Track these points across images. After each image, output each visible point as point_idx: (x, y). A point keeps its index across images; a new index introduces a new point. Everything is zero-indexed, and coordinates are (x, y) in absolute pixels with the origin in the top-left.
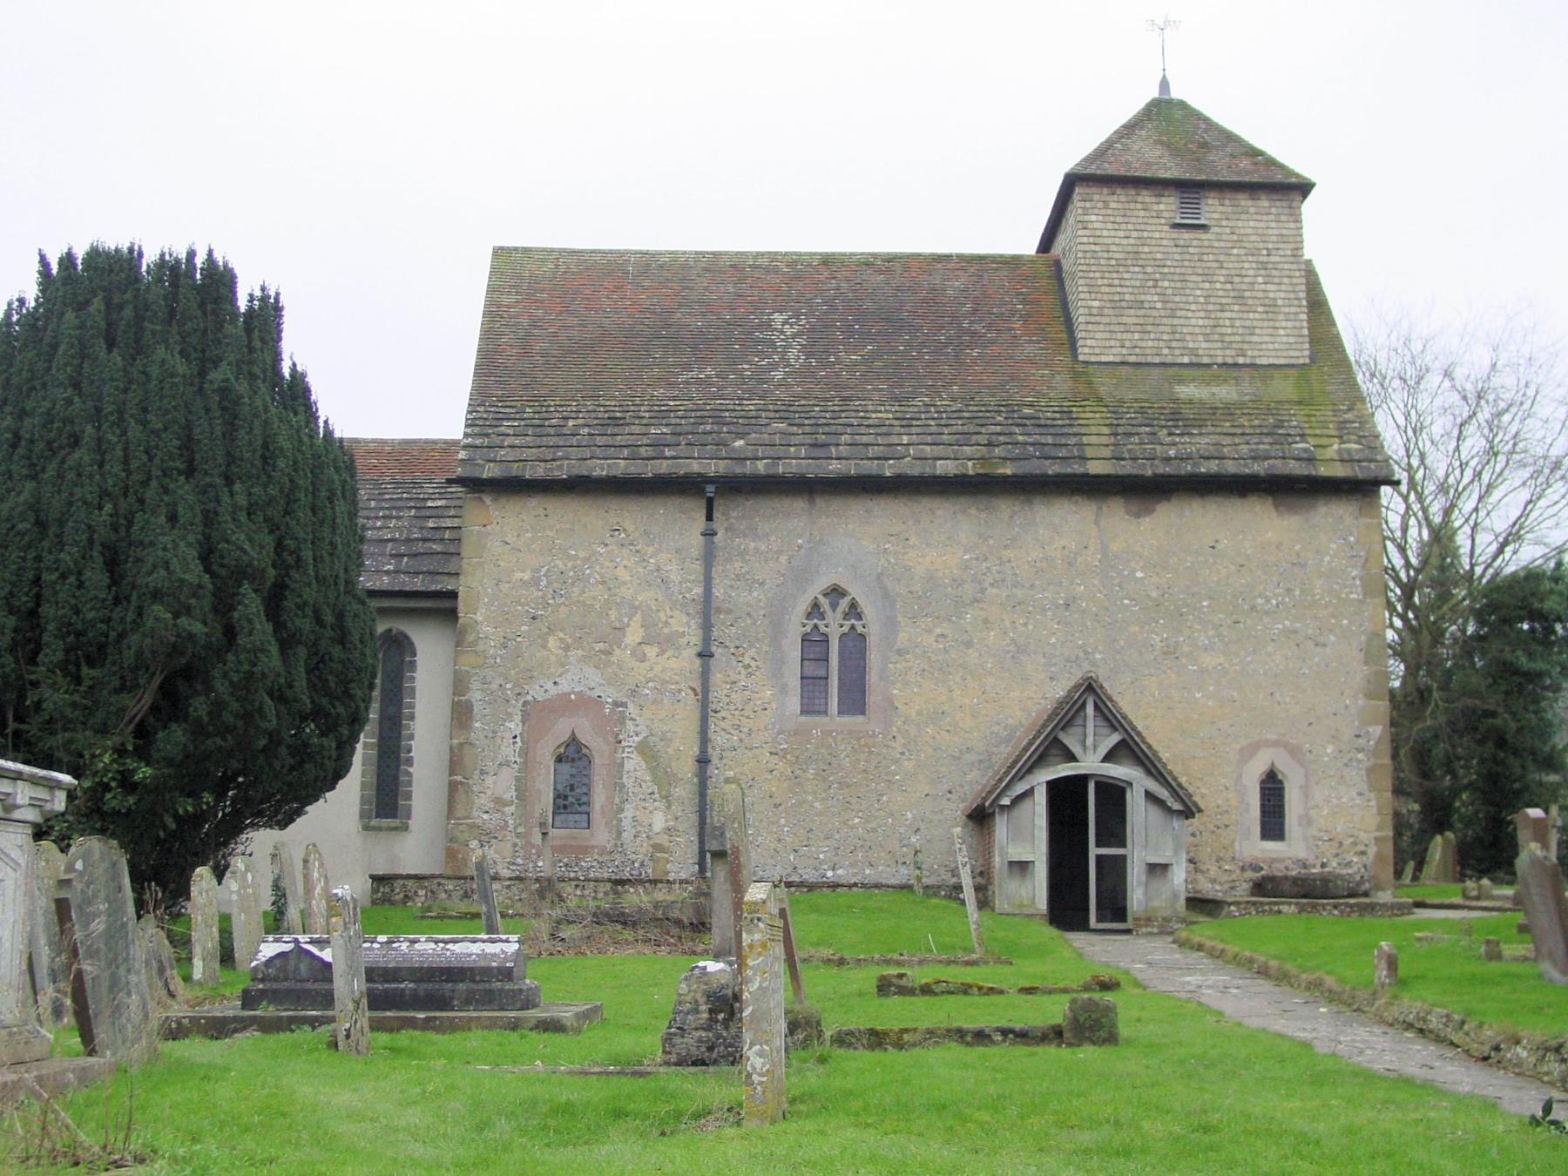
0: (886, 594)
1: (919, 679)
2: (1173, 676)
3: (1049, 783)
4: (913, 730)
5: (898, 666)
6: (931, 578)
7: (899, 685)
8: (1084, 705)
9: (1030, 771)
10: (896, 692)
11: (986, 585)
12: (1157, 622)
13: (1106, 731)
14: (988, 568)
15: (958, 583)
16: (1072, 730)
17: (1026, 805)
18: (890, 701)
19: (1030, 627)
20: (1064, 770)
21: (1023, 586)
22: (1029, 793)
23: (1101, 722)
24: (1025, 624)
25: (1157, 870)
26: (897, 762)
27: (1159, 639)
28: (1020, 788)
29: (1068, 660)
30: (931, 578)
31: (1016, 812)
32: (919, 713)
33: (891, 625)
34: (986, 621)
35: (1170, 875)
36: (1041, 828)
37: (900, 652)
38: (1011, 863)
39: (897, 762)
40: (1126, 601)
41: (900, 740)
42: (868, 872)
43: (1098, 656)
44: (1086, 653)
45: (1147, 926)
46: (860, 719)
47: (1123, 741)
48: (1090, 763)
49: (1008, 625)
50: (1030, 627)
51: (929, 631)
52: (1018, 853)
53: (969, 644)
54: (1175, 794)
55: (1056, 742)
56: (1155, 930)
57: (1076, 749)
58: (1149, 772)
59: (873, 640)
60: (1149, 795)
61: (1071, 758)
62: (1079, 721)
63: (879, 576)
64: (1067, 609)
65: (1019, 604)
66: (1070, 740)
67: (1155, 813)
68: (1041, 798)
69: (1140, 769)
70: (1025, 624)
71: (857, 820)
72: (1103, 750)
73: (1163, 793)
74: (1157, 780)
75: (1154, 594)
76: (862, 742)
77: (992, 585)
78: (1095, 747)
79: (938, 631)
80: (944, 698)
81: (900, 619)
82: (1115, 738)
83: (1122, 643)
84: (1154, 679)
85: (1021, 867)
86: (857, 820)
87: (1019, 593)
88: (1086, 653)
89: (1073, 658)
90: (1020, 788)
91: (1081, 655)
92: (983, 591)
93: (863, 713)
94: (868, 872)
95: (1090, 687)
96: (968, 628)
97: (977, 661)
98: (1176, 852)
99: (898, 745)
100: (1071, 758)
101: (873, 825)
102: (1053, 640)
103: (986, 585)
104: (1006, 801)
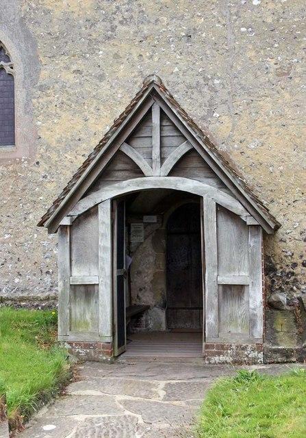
0: (28, 37)
1: (58, 110)
2: (287, 96)
3: (113, 200)
4: (54, 157)
5: (40, 100)
6: (68, 20)
7: (41, 118)
8: (150, 111)
9: (94, 187)
10: (39, 123)
11: (116, 23)
12: (273, 45)
13: (175, 141)
14: (118, 8)
15: (91, 23)
16: (137, 143)
17: (91, 224)
18: (35, 129)
19: (156, 59)
20: (129, 186)
21: (149, 22)
22: (92, 212)
23: (168, 131)
24: (151, 57)
25: (234, 291)
26: (40, 184)
27: (274, 61)
28: (83, 206)
29: (190, 87)
30: (68, 20)
31: (79, 234)
32: (59, 142)
33: (33, 63)
34: (116, 56)
35: (245, 298)
36: (104, 248)
37: (41, 88)
38: (74, 287)
39: (40, 184)
40: (243, 29)
41: (44, 166)
42: (17, 280)
43: (216, 82)
44: (206, 79)
45: (219, 354)
46: (9, 148)
47: (193, 150)
48: (156, 178)
49: (136, 59)
50: (156, 59)
51: (67, 68)
52: (81, 275)
53: (101, 78)
54: (248, 205)
55: (119, 152)
56: (229, 359)
57: (142, 164)
58: (222, 185)
59: (18, 79)
60: (221, 209)
61: (138, 172)
62: (145, 133)
63: (22, 19)
64: (188, 41)
65: (146, 38)
66: (134, 153)
67: (228, 229)
68: (105, 216)
69: (211, 181)
70: (151, 57)
71: (7, 236)
72: (170, 163)
73: (237, 207)
74: (234, 196)
75: (269, 20)
76: (11, 168)
77: (121, 22)
78: (162, 159)
79: (74, 67)
80: (80, 127)
81: (41, 58)
82: (183, 148)
83: (239, 68)
84: (268, 99)
85: (88, 291)
86: (7, 236)
87: (146, 29)
88: (206, 79)
89: (194, 84)
90: (83, 206)
91: (202, 81)
92: (113, 29)
93: (13, 143)
94: (17, 280)
95: (152, 93)
96: (101, 63)
97: (109, 92)
98: (252, 272)
99: (42, 170)
100: (138, 172)
101: (22, 240)
102: (176, 69)
103: (116, 23)
104: (66, 221)
